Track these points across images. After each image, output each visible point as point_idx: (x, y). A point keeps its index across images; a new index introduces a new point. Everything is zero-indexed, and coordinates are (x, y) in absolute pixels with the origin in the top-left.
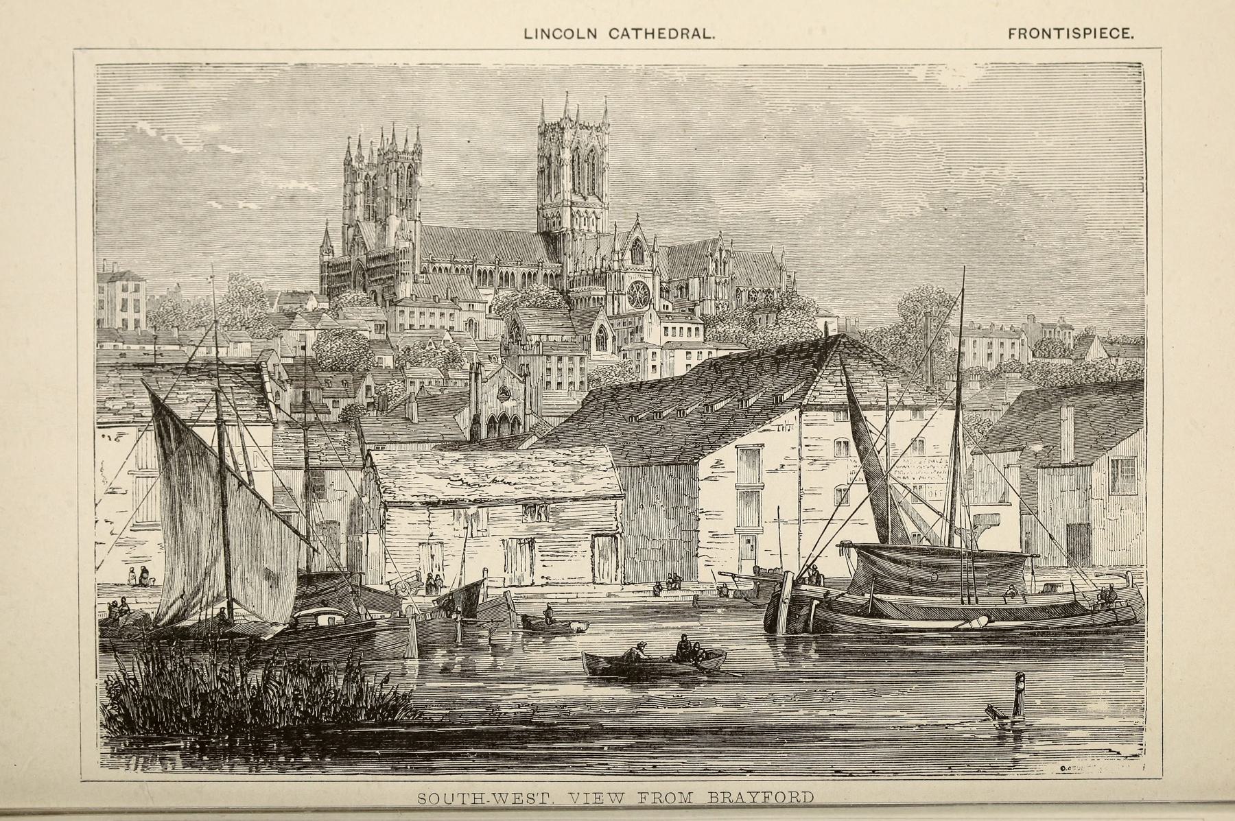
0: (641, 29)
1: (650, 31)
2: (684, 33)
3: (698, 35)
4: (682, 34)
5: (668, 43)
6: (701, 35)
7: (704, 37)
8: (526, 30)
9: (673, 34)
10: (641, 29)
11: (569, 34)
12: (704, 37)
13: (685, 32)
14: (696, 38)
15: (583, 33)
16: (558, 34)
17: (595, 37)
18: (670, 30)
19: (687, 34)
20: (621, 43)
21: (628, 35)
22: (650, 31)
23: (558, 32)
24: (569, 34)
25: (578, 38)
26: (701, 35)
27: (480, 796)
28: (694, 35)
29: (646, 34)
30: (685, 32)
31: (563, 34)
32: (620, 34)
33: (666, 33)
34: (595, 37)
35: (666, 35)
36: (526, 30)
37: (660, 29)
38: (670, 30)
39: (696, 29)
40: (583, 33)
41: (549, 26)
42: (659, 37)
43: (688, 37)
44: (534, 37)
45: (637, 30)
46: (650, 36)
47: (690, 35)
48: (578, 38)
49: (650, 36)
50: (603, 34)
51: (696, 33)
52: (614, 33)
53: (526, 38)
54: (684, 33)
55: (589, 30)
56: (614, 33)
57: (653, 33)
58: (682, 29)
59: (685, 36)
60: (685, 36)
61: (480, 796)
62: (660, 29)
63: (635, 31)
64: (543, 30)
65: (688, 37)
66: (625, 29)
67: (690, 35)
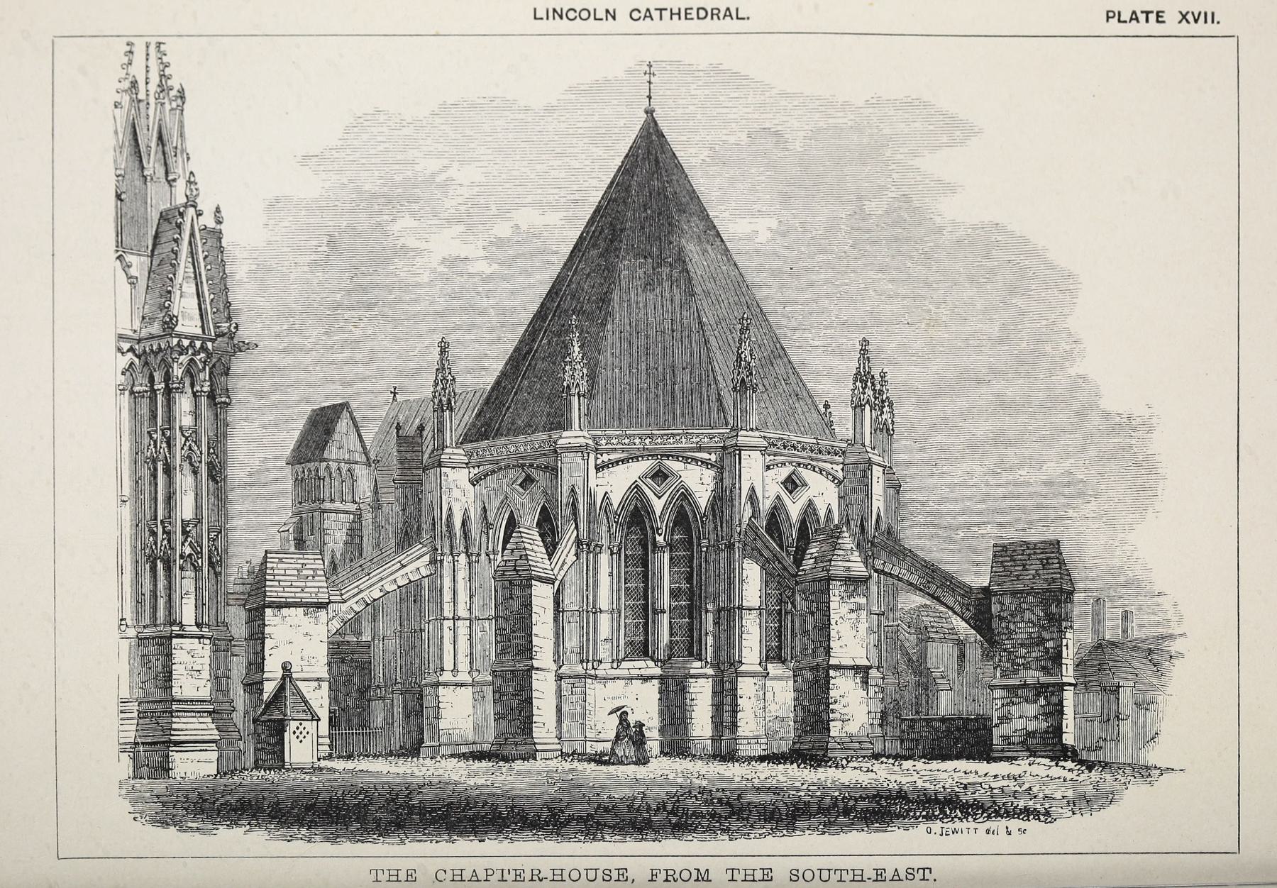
0: (666, 9)
1: (675, 11)
2: (714, 13)
3: (730, 15)
4: (712, 14)
5: (694, 25)
6: (734, 16)
7: (738, 18)
8: (535, 9)
9: (702, 14)
10: (666, 9)
12: (738, 18)
13: (715, 12)
14: (728, 18)
15: (600, 14)
16: (571, 15)
17: (614, 18)
18: (698, 9)
19: (717, 15)
21: (651, 16)
22: (675, 11)
23: (572, 12)
24: (585, 14)
25: (595, 19)
26: (734, 16)
28: (725, 15)
29: (672, 14)
30: (715, 12)
31: (577, 14)
32: (642, 15)
34: (614, 18)
35: (694, 12)
36: (535, 9)
37: (686, 9)
38: (698, 9)
40: (600, 14)
42: (686, 18)
43: (719, 18)
44: (545, 17)
45: (661, 10)
46: (675, 17)
47: (721, 15)
48: (595, 19)
49: (675, 17)
50: (623, 15)
51: (728, 13)
52: (636, 15)
53: (535, 18)
54: (714, 13)
55: (607, 11)
58: (712, 10)
59: (715, 17)
60: (715, 17)
62: (686, 9)
63: (659, 12)
64: (555, 10)
65: (719, 18)
66: (648, 10)
67: (721, 15)
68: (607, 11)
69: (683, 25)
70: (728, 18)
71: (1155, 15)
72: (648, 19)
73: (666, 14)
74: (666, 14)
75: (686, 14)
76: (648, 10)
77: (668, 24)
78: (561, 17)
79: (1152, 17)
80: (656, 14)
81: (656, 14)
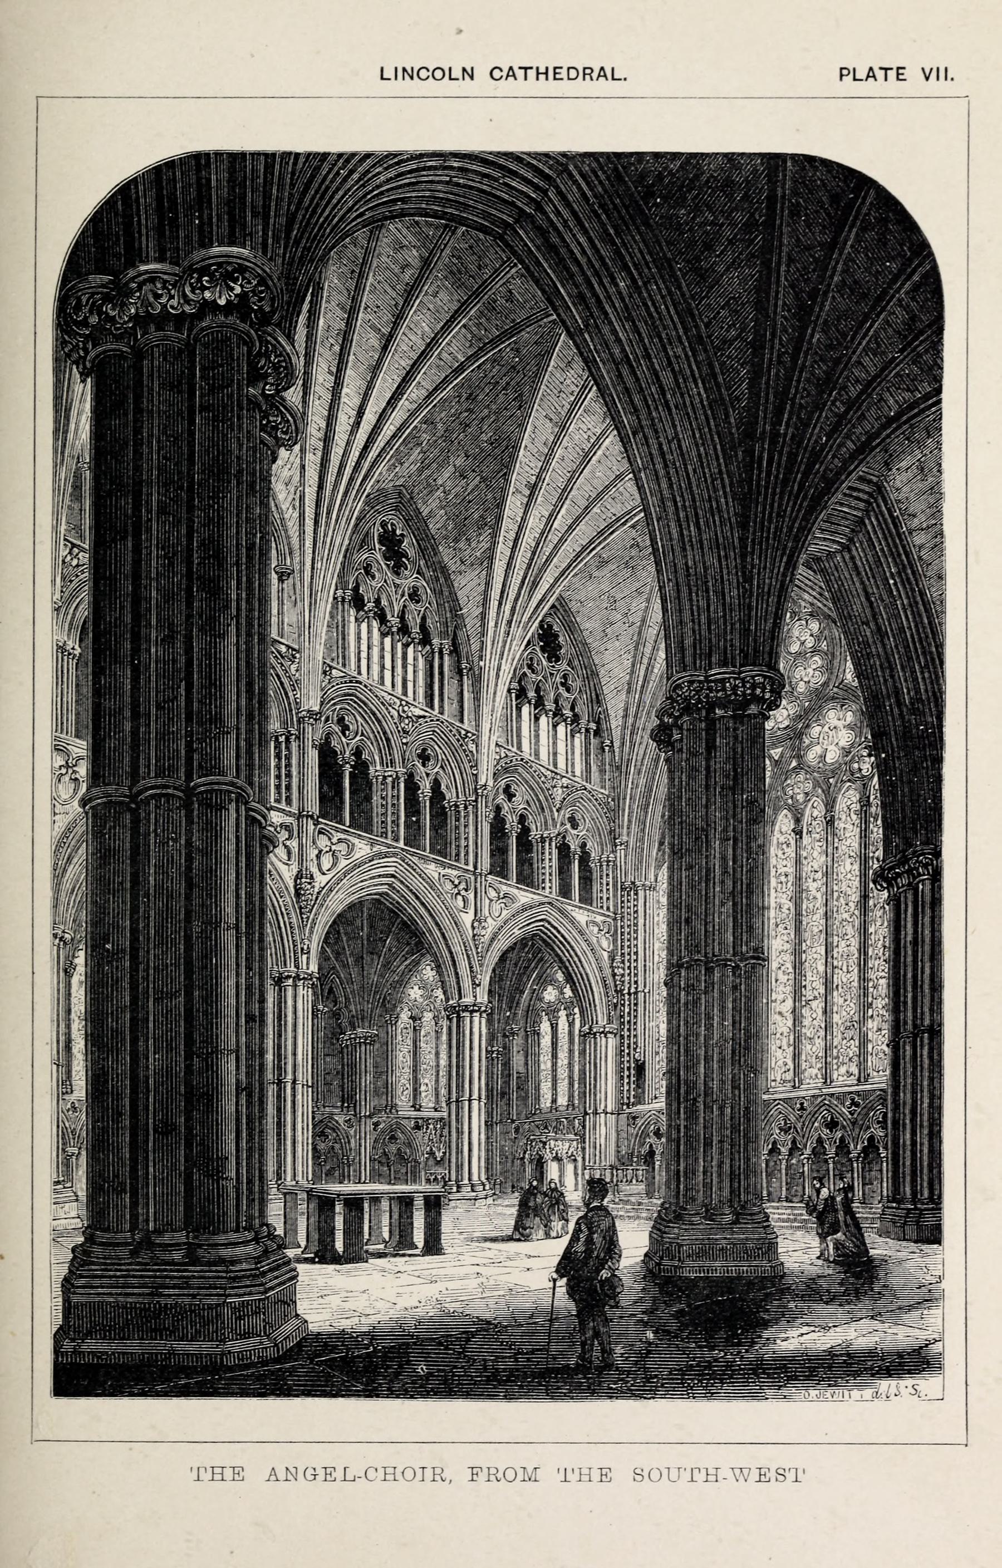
1: (542, 70)
3: (605, 76)
7: (613, 79)
9: (573, 74)
11: (438, 74)
13: (588, 71)
14: (602, 79)
15: (457, 73)
16: (423, 74)
17: (472, 77)
20: (508, 86)
21: (514, 75)
22: (542, 70)
24: (438, 74)
25: (451, 79)
27: (219, 1470)
29: (538, 73)
32: (504, 74)
33: (563, 73)
34: (472, 77)
35: (563, 73)
37: (555, 68)
39: (602, 69)
40: (457, 73)
41: (413, 62)
45: (526, 69)
46: (542, 77)
48: (451, 79)
49: (542, 77)
50: (482, 73)
52: (497, 74)
54: (587, 72)
55: (464, 70)
56: (497, 74)
57: (546, 73)
59: (587, 77)
60: (587, 77)
61: (219, 1470)
62: (555, 68)
66: (511, 68)
68: (464, 70)
69: (550, 87)
70: (602, 79)
71: (894, 72)
72: (511, 79)
73: (532, 73)
74: (532, 73)
75: (555, 73)
76: (511, 68)
77: (533, 86)
78: (412, 78)
79: (892, 74)
80: (520, 73)
81: (520, 73)
